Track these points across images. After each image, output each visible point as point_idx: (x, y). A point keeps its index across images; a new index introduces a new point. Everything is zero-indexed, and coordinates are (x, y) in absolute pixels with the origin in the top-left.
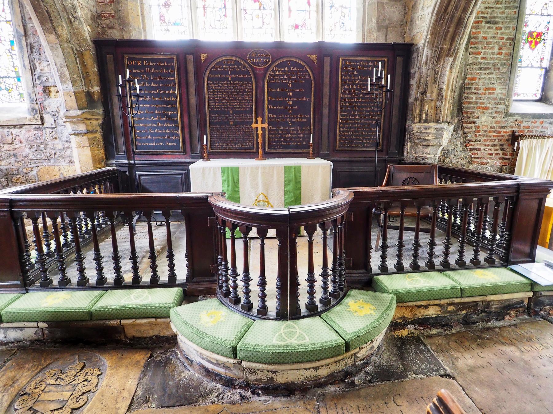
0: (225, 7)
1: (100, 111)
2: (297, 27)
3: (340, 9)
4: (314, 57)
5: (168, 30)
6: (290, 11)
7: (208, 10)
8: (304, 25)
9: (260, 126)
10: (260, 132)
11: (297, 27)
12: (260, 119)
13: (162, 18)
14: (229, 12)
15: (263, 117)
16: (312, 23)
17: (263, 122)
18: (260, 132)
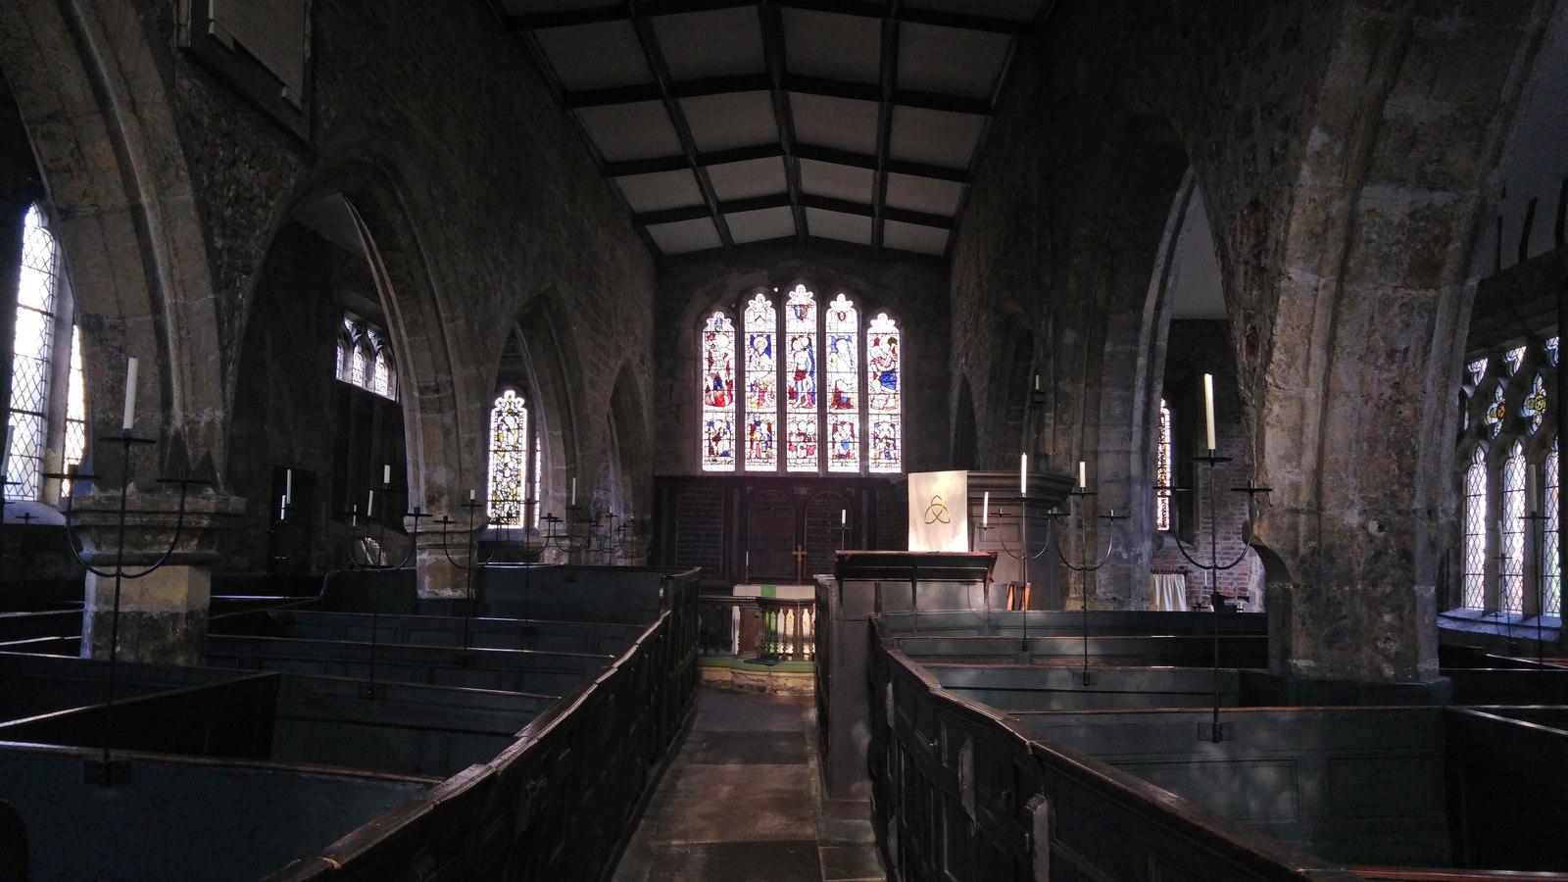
0: (771, 440)
1: (649, 536)
2: (840, 456)
3: (884, 440)
4: (852, 491)
5: (716, 460)
6: (834, 442)
7: (755, 443)
8: (848, 455)
9: (799, 553)
10: (800, 559)
11: (840, 456)
12: (800, 547)
13: (711, 451)
14: (775, 445)
15: (803, 546)
16: (856, 453)
17: (803, 550)
18: (800, 559)
